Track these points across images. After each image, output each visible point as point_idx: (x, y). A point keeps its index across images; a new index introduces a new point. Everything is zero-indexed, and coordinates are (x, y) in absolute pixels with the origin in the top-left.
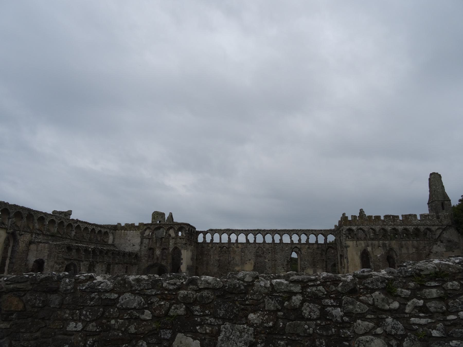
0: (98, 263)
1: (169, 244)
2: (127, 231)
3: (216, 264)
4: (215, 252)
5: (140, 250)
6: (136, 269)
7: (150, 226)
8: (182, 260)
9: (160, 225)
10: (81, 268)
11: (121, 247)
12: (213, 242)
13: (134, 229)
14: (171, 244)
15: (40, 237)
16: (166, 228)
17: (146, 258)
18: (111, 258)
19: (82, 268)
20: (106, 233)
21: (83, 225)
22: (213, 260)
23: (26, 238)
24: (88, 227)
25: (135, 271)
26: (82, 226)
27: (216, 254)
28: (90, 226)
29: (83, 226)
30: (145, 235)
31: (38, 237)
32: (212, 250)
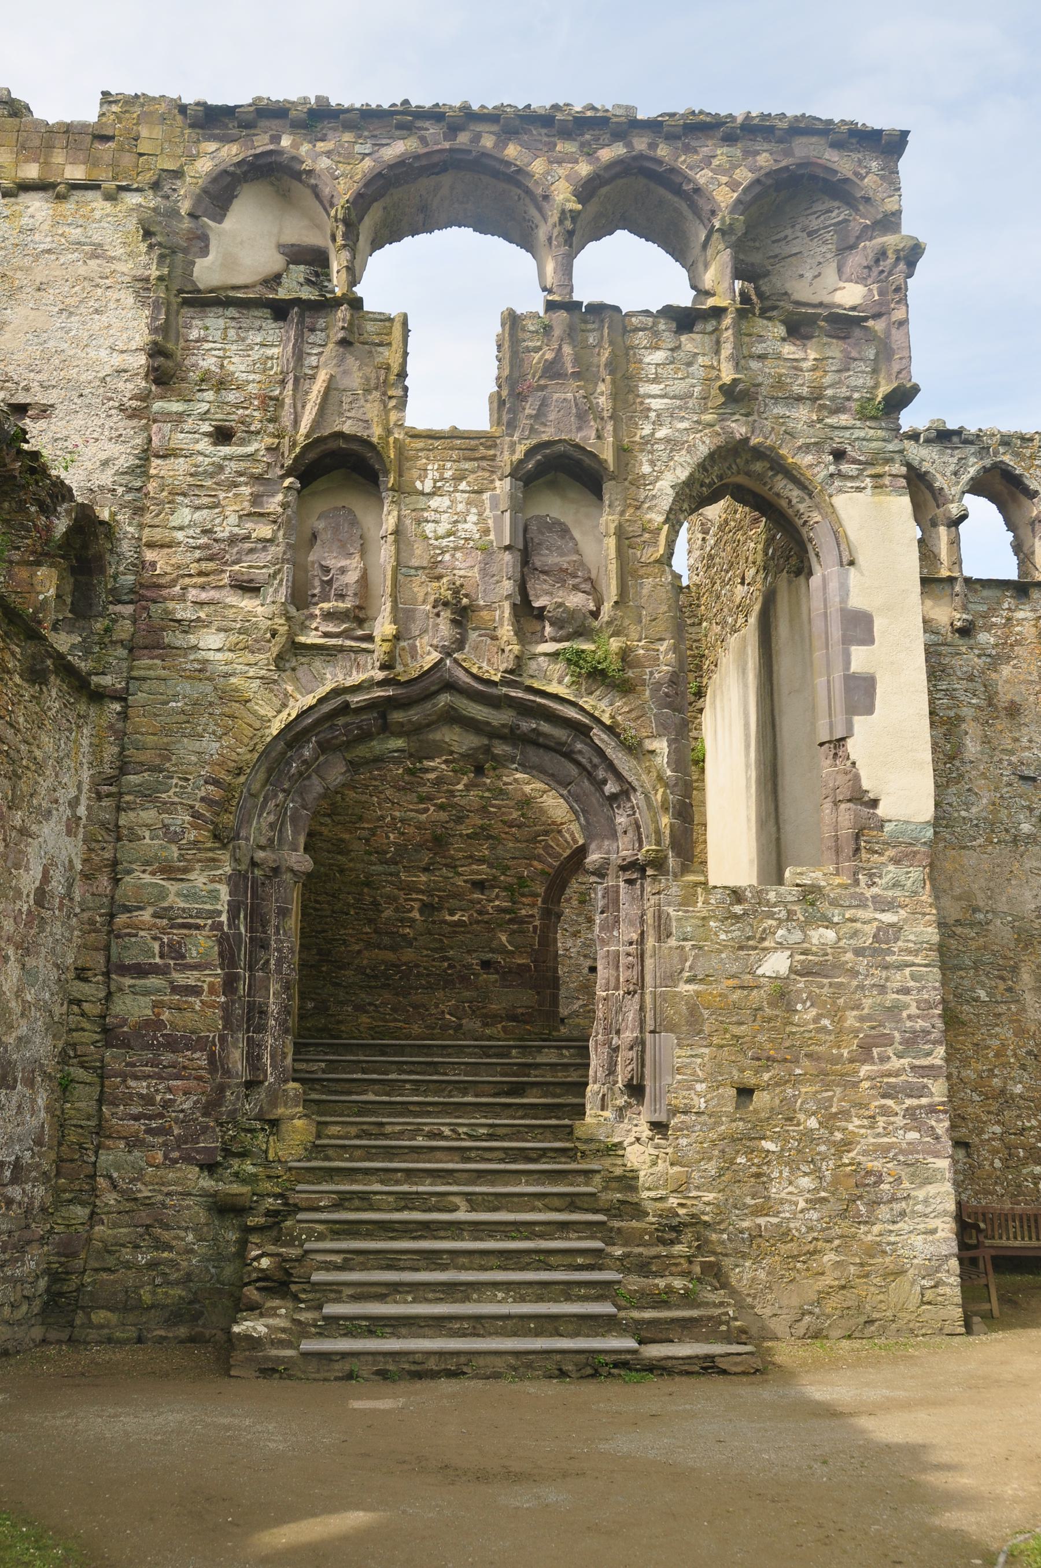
3: (1026, 828)
6: (86, 775)
7: (286, 142)
8: (869, 640)
13: (32, 172)
14: (656, 404)
16: (561, 171)
25: (74, 803)
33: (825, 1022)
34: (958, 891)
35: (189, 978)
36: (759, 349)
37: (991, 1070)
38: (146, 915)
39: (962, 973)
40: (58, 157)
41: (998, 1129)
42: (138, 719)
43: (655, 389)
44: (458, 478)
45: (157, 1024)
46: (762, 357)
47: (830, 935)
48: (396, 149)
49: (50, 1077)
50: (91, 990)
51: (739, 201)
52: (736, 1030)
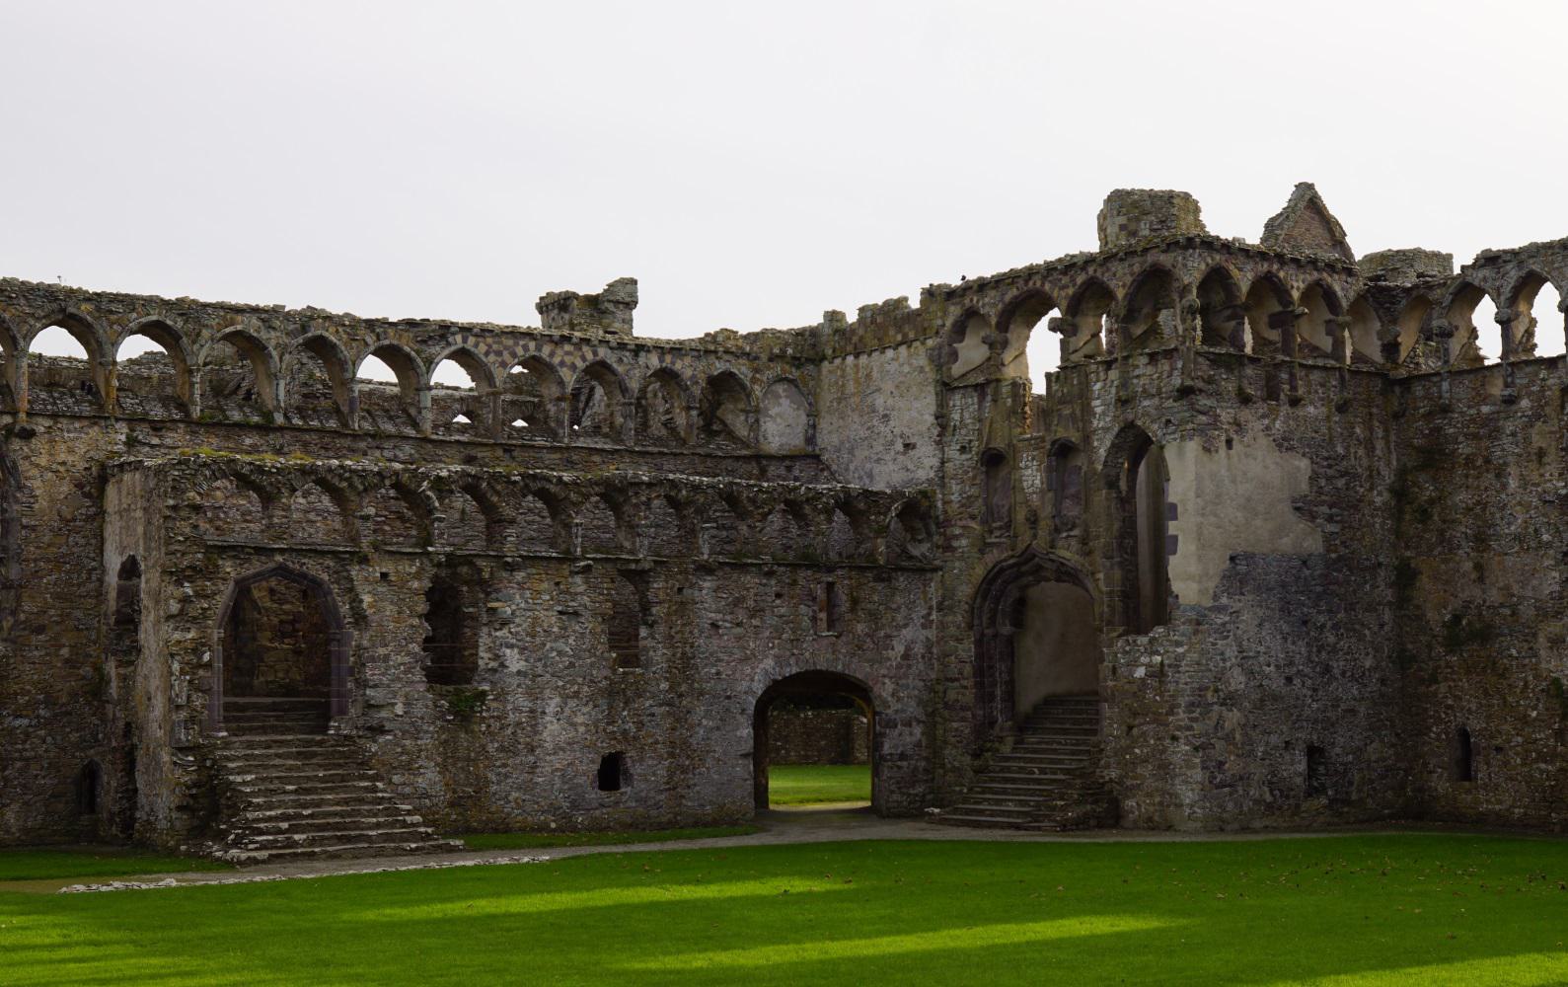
0: (511, 568)
1: (1087, 410)
2: (870, 355)
4: (1537, 442)
5: (942, 478)
7: (975, 299)
8: (1175, 518)
9: (1026, 282)
10: (361, 601)
11: (852, 467)
12: (1538, 353)
13: (899, 338)
14: (1098, 410)
15: (168, 441)
16: (1063, 294)
17: (973, 525)
18: (639, 535)
19: (367, 599)
20: (723, 386)
21: (495, 347)
22: (1520, 503)
23: (71, 451)
24: (552, 354)
26: (492, 358)
27: (1541, 454)
28: (568, 353)
29: (499, 353)
30: (957, 369)
31: (155, 441)
32: (1509, 427)
33: (1158, 698)
34: (1501, 584)
35: (965, 683)
36: (1137, 372)
37: (1518, 702)
38: (953, 658)
39: (1503, 639)
40: (906, 329)
41: (1520, 739)
42: (946, 575)
43: (1098, 402)
44: (1033, 459)
45: (957, 701)
46: (1138, 377)
47: (1159, 658)
48: (1014, 292)
49: (923, 722)
50: (940, 688)
51: (1126, 294)
52: (1126, 701)
